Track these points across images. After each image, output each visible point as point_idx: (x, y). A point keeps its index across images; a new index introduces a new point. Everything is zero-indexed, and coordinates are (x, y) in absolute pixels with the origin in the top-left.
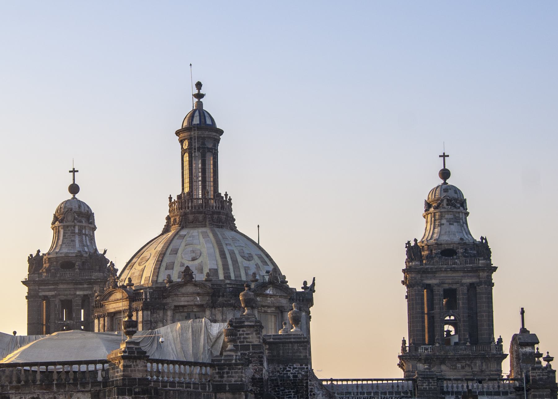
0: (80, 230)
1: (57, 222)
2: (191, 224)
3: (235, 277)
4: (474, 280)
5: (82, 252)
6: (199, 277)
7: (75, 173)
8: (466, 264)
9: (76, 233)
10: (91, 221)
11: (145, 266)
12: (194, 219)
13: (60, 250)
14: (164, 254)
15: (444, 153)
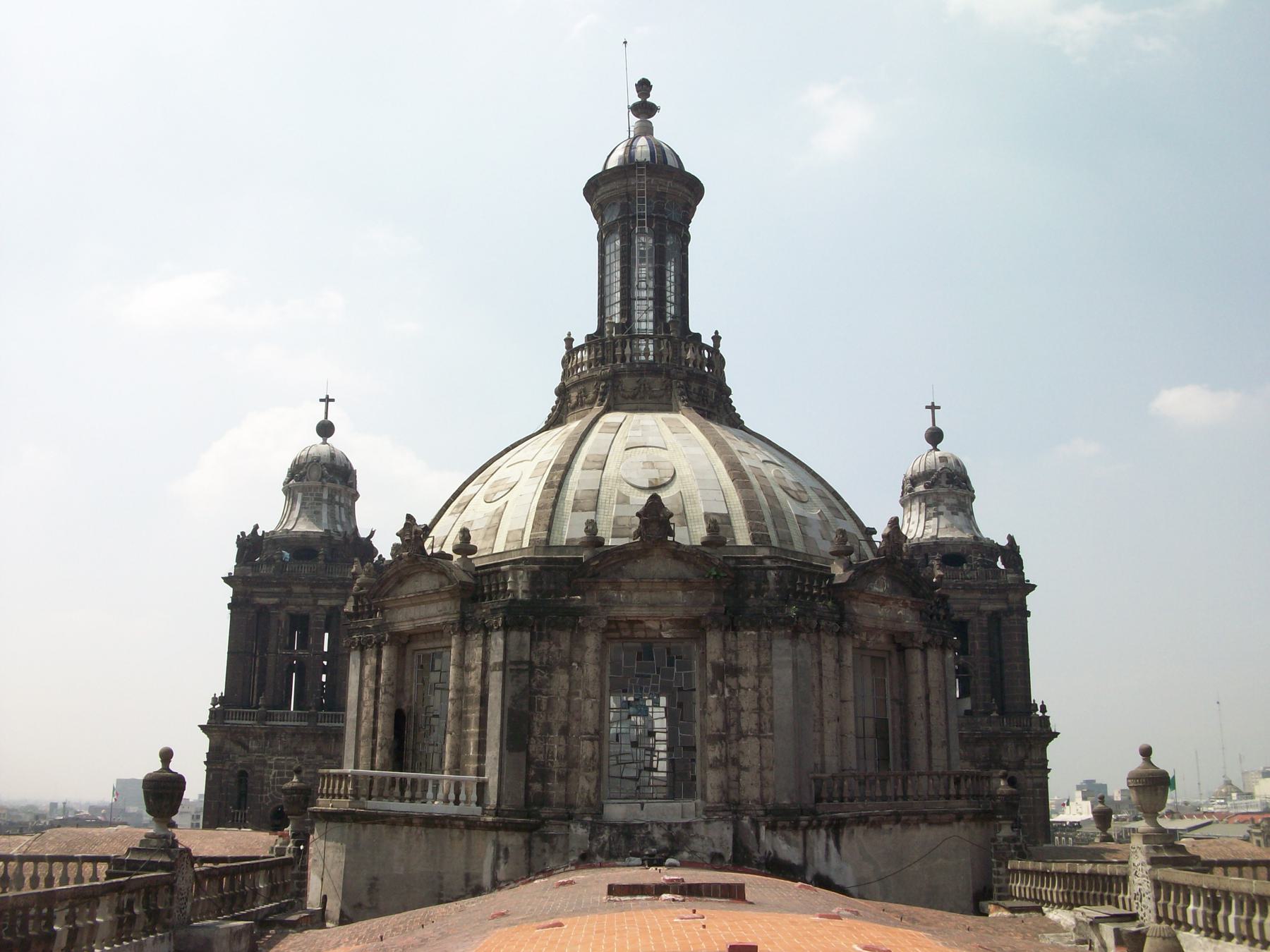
0: (331, 496)
1: (293, 480)
2: (630, 400)
3: (780, 541)
4: (999, 606)
5: (332, 532)
6: (691, 533)
7: (330, 403)
8: (986, 579)
9: (325, 500)
10: (351, 481)
11: (507, 503)
12: (640, 388)
13: (293, 527)
14: (568, 468)
15: (933, 403)
